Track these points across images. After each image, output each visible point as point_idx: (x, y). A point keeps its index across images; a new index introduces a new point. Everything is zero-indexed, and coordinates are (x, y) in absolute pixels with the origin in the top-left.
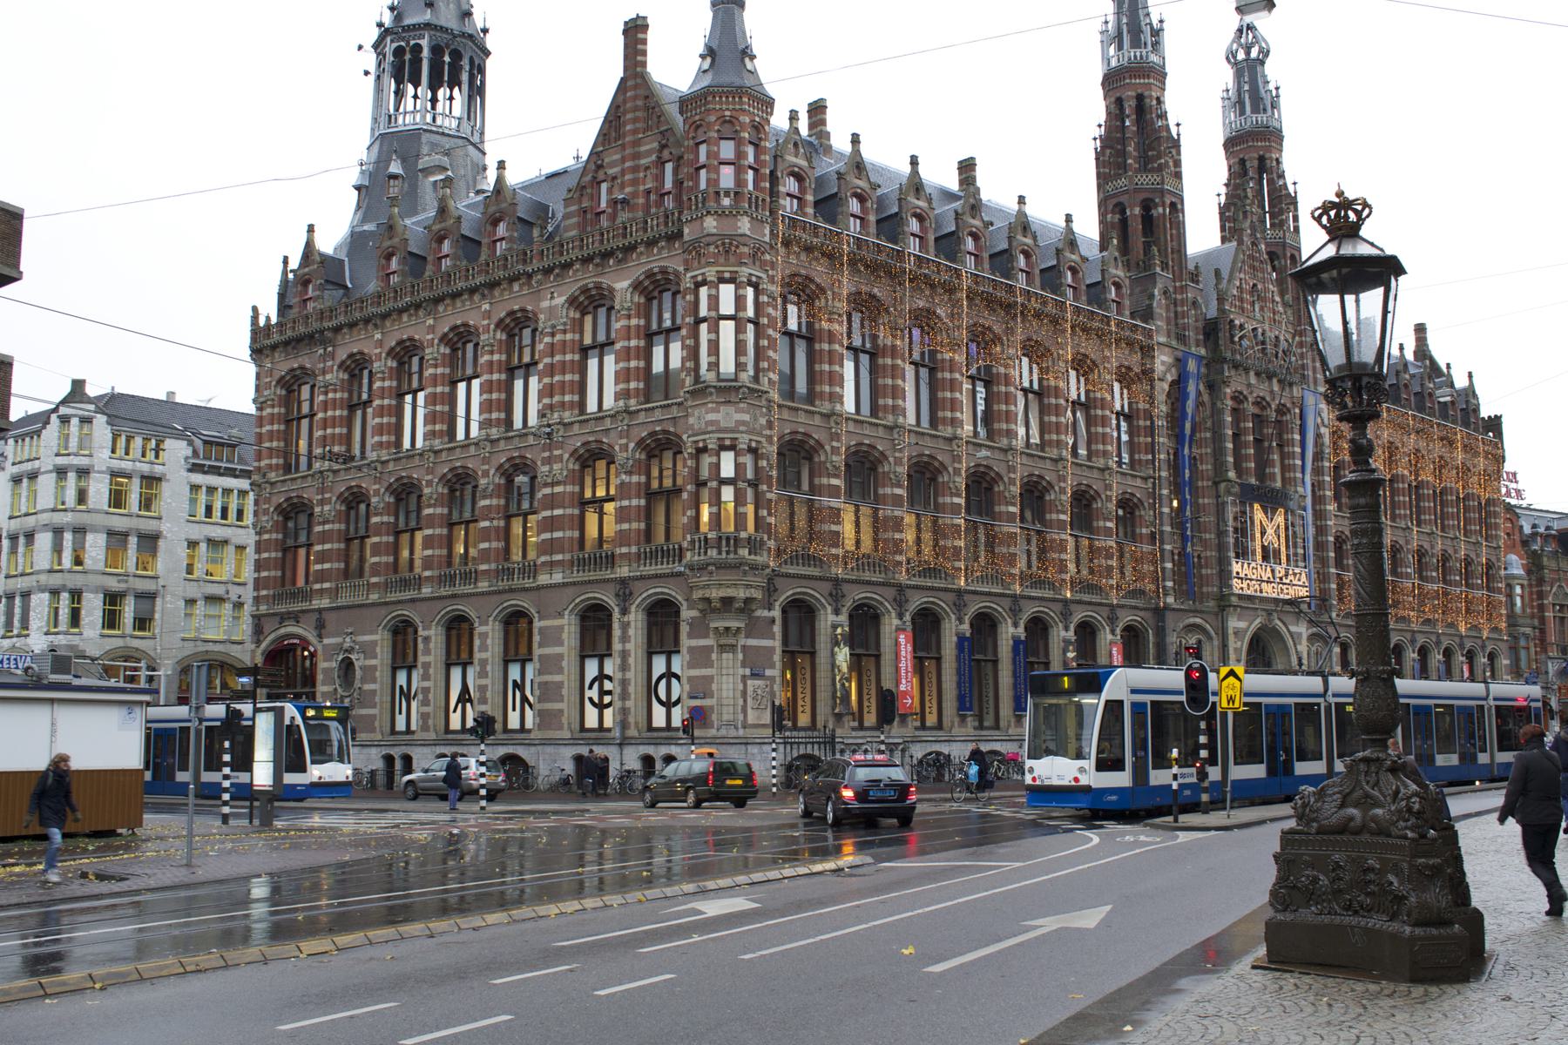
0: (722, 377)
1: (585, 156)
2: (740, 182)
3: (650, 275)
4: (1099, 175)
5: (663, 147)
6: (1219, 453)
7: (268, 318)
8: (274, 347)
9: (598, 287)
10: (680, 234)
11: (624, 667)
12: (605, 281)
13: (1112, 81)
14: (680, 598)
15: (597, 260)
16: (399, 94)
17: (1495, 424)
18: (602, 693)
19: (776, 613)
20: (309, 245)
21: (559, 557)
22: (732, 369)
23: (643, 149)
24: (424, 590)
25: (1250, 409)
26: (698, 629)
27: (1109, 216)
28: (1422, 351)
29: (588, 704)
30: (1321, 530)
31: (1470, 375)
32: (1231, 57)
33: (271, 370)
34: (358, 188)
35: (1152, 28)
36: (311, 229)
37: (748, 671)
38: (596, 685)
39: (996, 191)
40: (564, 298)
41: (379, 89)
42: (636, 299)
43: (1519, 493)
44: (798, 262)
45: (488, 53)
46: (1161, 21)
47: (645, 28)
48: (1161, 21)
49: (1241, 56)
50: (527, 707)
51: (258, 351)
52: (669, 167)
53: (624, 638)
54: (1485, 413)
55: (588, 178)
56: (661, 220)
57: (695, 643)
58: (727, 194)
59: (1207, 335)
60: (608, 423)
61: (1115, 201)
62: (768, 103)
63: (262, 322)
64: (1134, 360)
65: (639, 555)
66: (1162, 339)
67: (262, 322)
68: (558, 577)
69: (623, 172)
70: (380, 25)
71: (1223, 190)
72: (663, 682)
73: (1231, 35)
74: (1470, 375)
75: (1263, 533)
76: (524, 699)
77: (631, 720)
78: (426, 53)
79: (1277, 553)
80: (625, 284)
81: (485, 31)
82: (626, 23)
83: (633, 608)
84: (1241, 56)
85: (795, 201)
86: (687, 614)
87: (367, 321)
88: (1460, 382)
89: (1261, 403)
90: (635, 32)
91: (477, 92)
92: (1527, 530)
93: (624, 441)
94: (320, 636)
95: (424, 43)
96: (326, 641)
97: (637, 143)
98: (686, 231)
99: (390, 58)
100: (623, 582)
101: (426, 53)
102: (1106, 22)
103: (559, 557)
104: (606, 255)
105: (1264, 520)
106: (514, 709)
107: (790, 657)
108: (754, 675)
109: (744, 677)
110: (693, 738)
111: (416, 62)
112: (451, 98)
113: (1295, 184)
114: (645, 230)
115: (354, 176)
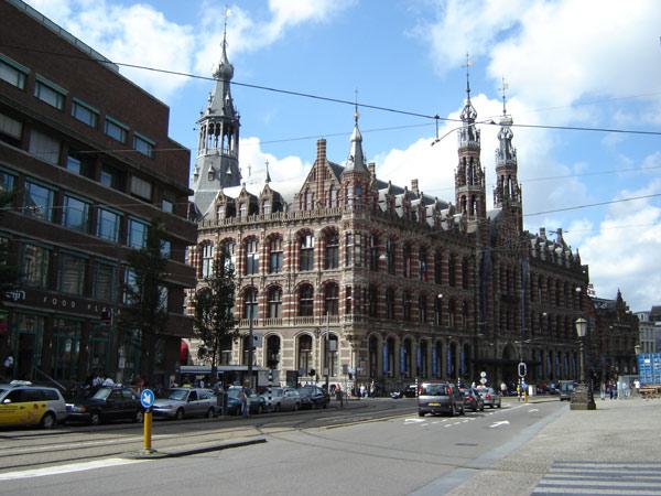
3: (328, 228)
6: (495, 283)
10: (340, 217)
17: (586, 268)
25: (506, 268)
30: (526, 310)
32: (500, 138)
43: (594, 293)
44: (375, 225)
49: (503, 137)
64: (468, 251)
68: (292, 325)
88: (574, 253)
90: (322, 144)
92: (596, 307)
100: (317, 328)
104: (312, 220)
107: (371, 353)
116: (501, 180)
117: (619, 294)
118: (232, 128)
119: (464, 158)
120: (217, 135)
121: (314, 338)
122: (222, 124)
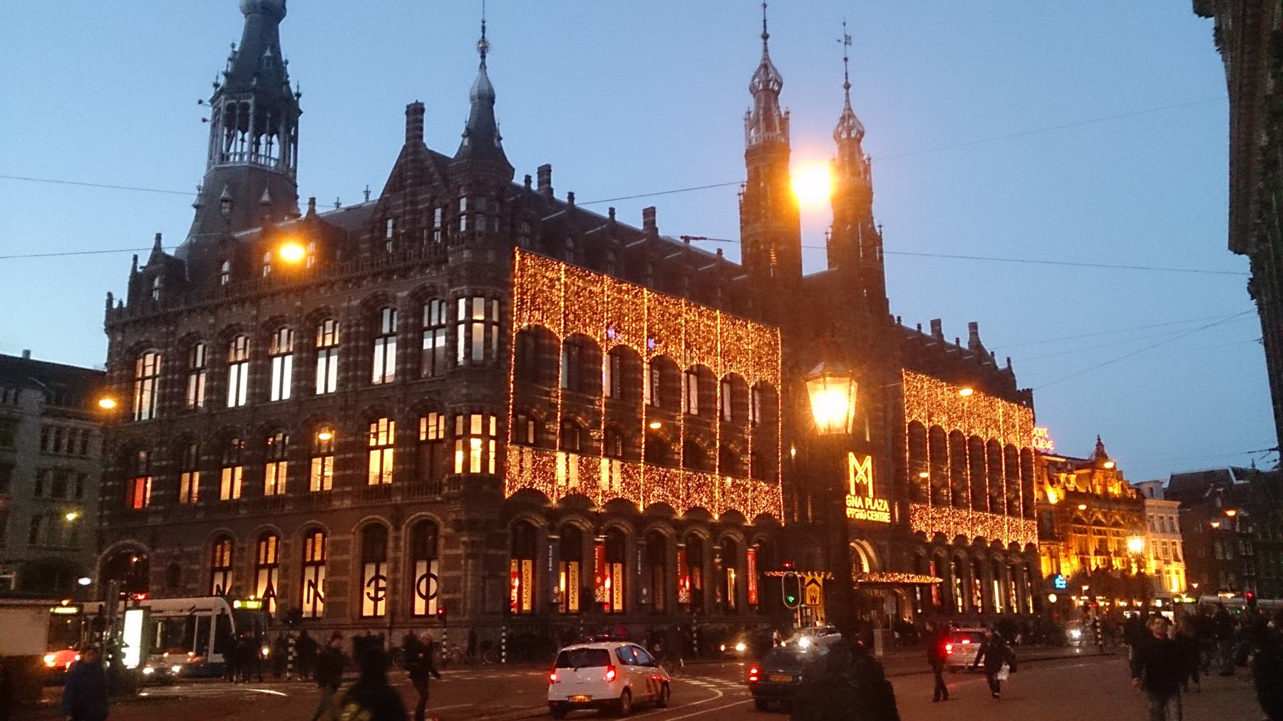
0: (474, 363)
1: (376, 195)
2: (489, 227)
3: (423, 288)
4: (742, 221)
5: (434, 198)
7: (121, 303)
8: (126, 324)
9: (385, 294)
11: (395, 570)
12: (390, 291)
14: (438, 519)
16: (230, 137)
18: (377, 589)
19: (509, 531)
20: (157, 248)
21: (348, 489)
22: (481, 357)
23: (419, 198)
24: (242, 512)
26: (451, 542)
27: (749, 249)
28: (976, 343)
29: (365, 597)
31: (1009, 360)
33: (121, 343)
34: (196, 207)
35: (781, 118)
36: (159, 237)
37: (487, 573)
38: (373, 584)
40: (359, 301)
41: (214, 135)
42: (412, 304)
47: (423, 110)
48: (787, 113)
50: (318, 599)
51: (110, 329)
52: (438, 212)
53: (397, 548)
54: (1020, 387)
55: (379, 216)
56: (432, 250)
57: (448, 552)
58: (480, 234)
60: (389, 392)
61: (752, 239)
62: (510, 171)
63: (115, 305)
65: (409, 488)
67: (115, 305)
69: (404, 213)
70: (216, 85)
71: (830, 230)
72: (424, 580)
74: (1009, 360)
75: (856, 473)
76: (316, 594)
77: (399, 608)
78: (251, 110)
79: (866, 487)
80: (405, 293)
81: (299, 95)
82: (408, 106)
83: (404, 527)
84: (844, 136)
85: (528, 240)
86: (444, 530)
87: (204, 309)
88: (1001, 364)
90: (415, 113)
91: (291, 140)
93: (402, 405)
94: (153, 548)
95: (251, 101)
96: (158, 551)
97: (414, 194)
98: (450, 259)
99: (223, 111)
100: (397, 507)
101: (251, 110)
102: (749, 113)
103: (348, 489)
105: (857, 465)
106: (308, 602)
108: (491, 576)
109: (484, 578)
110: (445, 622)
111: (245, 115)
112: (271, 143)
113: (880, 226)
114: (420, 257)
115: (194, 199)
117: (1100, 445)
121: (391, 528)
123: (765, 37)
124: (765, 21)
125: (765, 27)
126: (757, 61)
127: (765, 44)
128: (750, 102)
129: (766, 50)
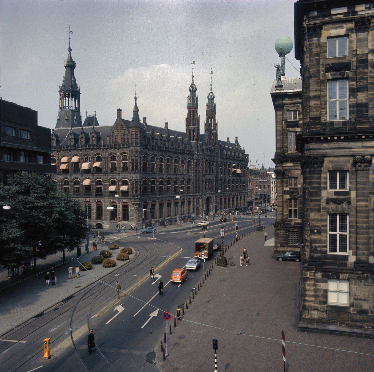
13: (189, 108)
15: (114, 149)
17: (248, 155)
28: (237, 142)
31: (244, 148)
39: (170, 127)
45: (80, 93)
46: (198, 97)
49: (210, 97)
53: (119, 207)
54: (246, 154)
59: (202, 151)
66: (195, 153)
70: (60, 87)
73: (208, 94)
74: (244, 148)
80: (119, 153)
81: (80, 89)
88: (243, 149)
89: (210, 161)
90: (119, 111)
112: (72, 100)
116: (208, 118)
117: (263, 166)
118: (76, 96)
119: (190, 111)
120: (69, 97)
121: (118, 203)
122: (70, 94)
123: (193, 77)
124: (193, 73)
125: (193, 74)
126: (191, 83)
127: (193, 78)
128: (188, 93)
129: (193, 80)
